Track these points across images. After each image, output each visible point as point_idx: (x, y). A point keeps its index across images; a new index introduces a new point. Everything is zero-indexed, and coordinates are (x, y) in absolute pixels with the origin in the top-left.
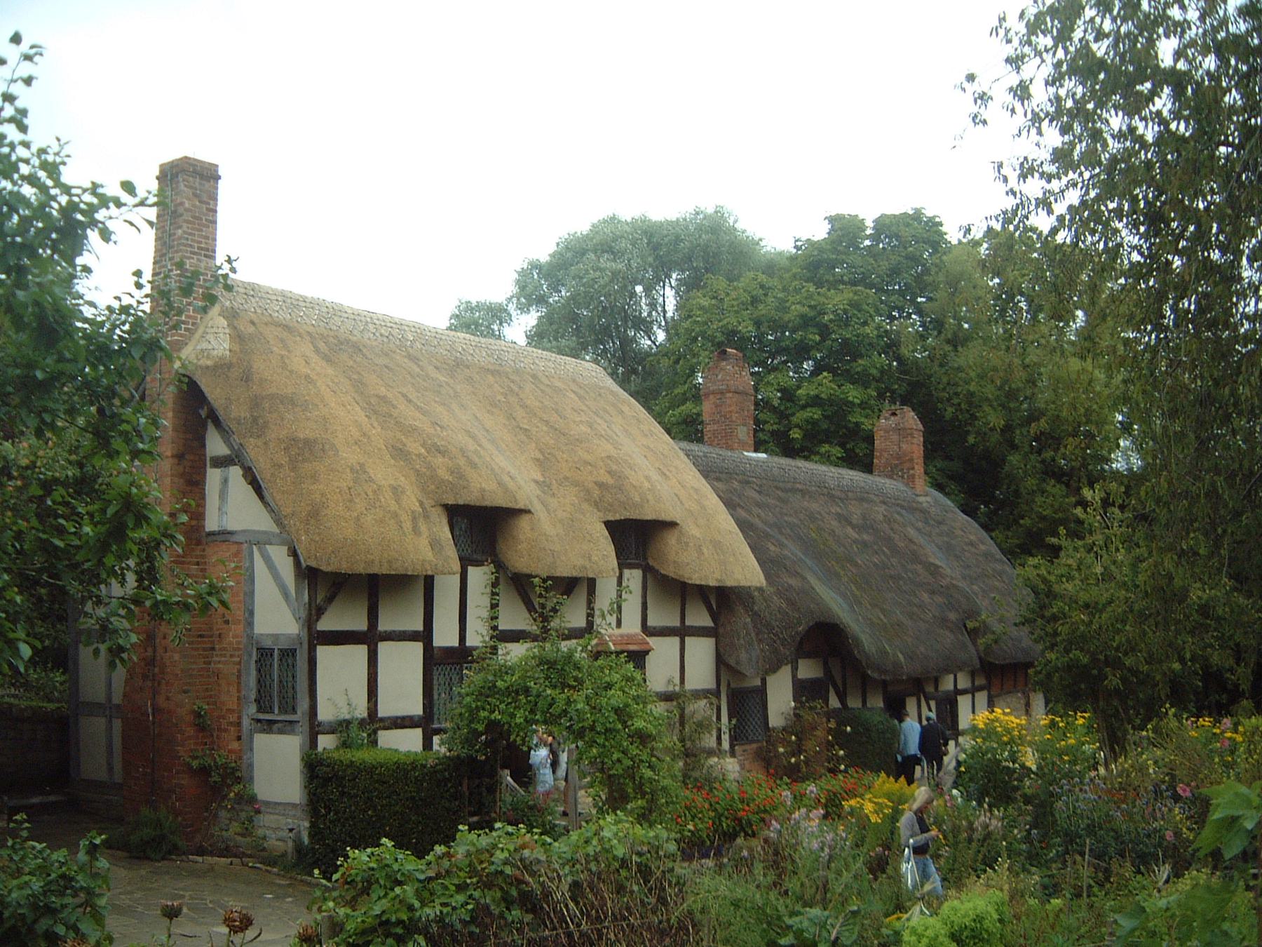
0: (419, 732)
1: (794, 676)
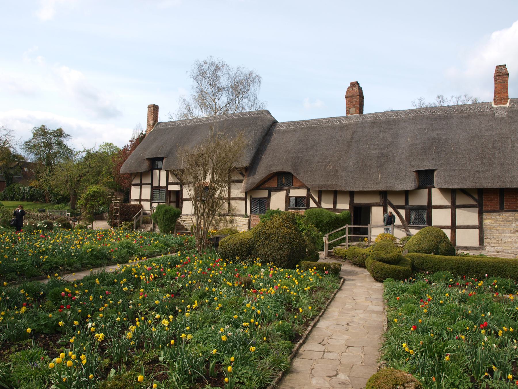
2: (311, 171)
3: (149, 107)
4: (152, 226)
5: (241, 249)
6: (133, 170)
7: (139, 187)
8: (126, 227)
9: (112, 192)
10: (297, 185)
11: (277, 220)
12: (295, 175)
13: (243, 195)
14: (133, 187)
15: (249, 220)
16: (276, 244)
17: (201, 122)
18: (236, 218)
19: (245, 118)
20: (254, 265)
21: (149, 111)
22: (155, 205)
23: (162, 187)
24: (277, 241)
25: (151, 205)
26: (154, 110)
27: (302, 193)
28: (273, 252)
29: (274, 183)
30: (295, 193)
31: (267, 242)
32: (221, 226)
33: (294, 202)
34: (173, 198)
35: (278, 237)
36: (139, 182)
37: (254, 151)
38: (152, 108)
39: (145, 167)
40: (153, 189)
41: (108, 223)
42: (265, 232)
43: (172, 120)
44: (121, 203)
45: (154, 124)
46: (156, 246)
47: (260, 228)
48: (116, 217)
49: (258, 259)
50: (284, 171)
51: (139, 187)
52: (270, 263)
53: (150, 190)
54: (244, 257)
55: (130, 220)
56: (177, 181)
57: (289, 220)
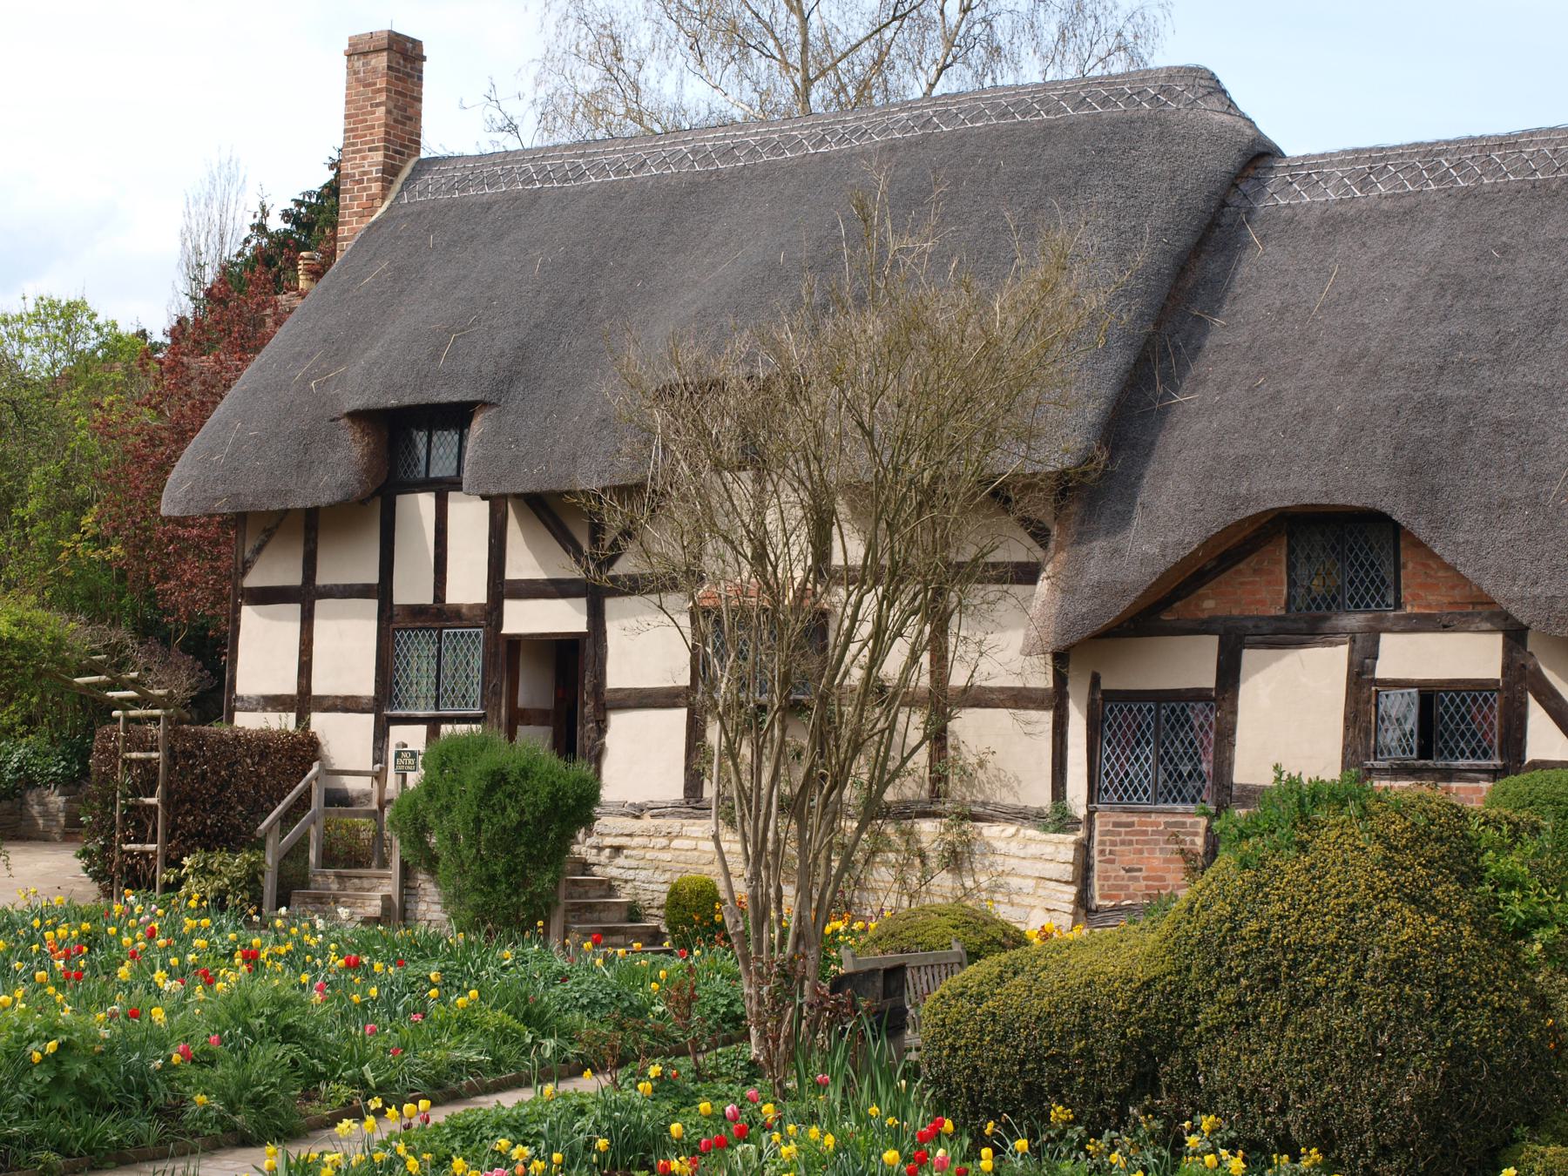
0: (370, 719)
2: (1535, 502)
3: (358, 51)
4: (390, 887)
5: (1087, 1054)
6: (257, 488)
7: (296, 609)
8: (211, 886)
9: (111, 649)
10: (1435, 600)
11: (1348, 855)
12: (1421, 531)
13: (1042, 679)
14: (248, 614)
15: (1084, 848)
16: (1343, 1018)
17: (727, 153)
18: (990, 831)
19: (1048, 130)
20: (1187, 1163)
21: (357, 80)
22: (411, 737)
23: (456, 615)
24: (1352, 997)
25: (381, 736)
26: (393, 70)
27: (1474, 656)
28: (1320, 1075)
29: (1265, 590)
30: (1410, 657)
31: (1277, 1003)
32: (883, 892)
33: (1411, 723)
34: (532, 690)
35: (1358, 973)
36: (288, 574)
37: (1117, 361)
38: (381, 61)
39: (341, 476)
40: (397, 625)
41: (80, 864)
42: (1263, 933)
43: (512, 144)
44: (174, 722)
45: (390, 172)
46: (465, 1025)
47: (1221, 908)
48: (139, 822)
49: (1207, 1122)
50: (1340, 500)
51: (296, 609)
52: (1295, 1158)
53: (373, 626)
54: (1109, 1104)
55: (236, 838)
56: (566, 568)
57: (1432, 850)
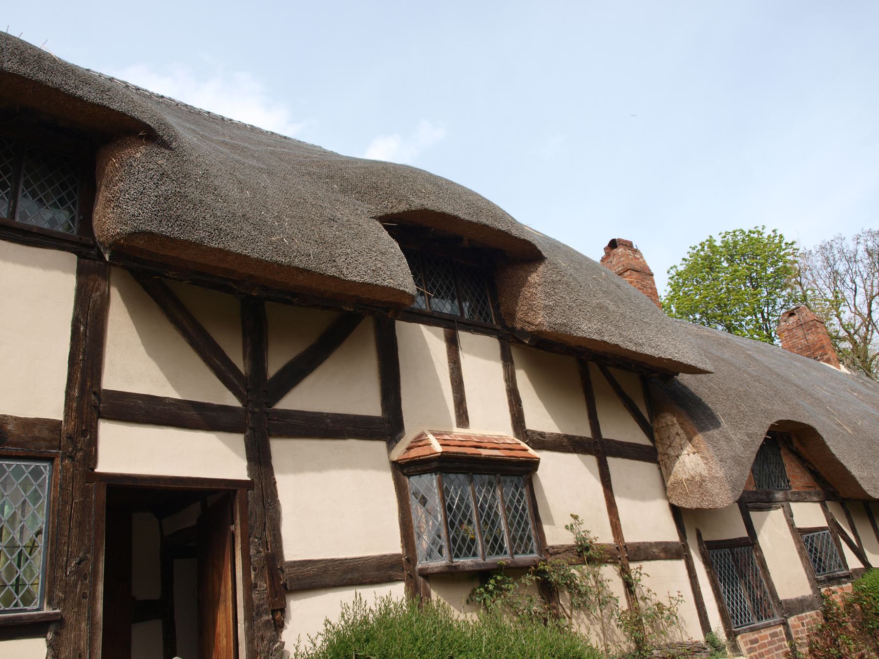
1: (791, 524)
